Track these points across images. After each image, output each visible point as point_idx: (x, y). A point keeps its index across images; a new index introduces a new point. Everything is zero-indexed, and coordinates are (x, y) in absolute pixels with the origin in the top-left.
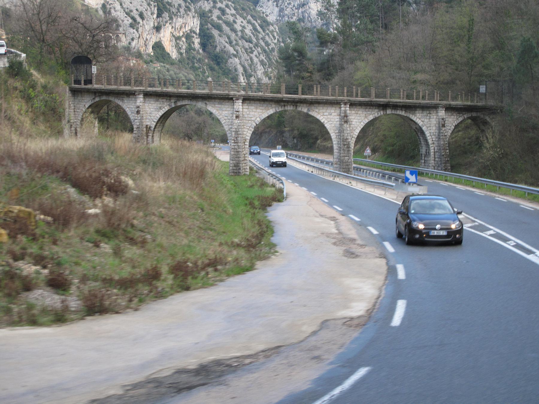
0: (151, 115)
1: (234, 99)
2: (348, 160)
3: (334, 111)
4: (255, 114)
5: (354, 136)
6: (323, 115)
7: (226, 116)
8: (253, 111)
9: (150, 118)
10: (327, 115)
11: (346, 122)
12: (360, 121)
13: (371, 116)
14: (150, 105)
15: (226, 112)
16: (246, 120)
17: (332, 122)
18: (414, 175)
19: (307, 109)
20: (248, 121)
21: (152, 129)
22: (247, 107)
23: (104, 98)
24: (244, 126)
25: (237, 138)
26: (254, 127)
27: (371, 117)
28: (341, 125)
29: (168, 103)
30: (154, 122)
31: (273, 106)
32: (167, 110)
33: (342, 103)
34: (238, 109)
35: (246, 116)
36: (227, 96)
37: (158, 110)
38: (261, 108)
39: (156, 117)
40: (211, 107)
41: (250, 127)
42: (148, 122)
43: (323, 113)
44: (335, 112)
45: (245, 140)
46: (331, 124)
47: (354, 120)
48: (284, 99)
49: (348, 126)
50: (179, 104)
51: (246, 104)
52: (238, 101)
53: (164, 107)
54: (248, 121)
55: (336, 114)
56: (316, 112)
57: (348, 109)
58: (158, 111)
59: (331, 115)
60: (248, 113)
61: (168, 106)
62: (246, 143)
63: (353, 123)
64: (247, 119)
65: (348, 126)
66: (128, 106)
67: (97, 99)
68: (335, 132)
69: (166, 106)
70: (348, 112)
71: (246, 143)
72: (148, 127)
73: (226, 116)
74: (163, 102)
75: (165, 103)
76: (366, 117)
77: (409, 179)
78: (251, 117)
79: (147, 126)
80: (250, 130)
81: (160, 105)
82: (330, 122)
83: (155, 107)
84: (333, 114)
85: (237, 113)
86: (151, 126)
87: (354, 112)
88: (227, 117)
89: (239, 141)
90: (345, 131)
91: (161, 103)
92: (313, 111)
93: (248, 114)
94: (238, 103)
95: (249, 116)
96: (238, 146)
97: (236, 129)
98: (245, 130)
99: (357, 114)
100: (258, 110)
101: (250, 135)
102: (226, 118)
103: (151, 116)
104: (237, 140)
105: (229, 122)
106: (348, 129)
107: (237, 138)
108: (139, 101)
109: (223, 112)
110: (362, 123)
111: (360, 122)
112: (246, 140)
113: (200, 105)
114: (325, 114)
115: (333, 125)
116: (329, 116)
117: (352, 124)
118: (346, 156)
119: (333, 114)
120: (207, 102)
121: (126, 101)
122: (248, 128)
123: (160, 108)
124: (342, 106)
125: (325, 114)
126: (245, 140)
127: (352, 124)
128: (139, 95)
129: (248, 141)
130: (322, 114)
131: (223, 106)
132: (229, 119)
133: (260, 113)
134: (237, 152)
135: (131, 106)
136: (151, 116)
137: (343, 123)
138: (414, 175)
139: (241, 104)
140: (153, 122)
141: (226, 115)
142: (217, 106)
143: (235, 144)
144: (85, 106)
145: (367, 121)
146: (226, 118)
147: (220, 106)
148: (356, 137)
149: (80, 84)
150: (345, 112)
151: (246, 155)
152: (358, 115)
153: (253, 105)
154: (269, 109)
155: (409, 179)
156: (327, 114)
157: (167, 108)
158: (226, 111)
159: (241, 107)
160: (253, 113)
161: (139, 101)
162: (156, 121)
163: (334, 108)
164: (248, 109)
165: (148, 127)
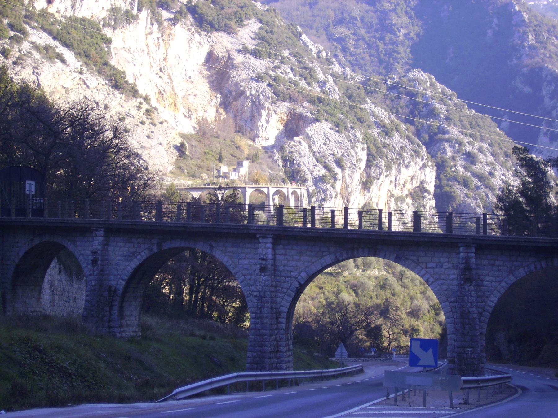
0: (118, 267)
1: (257, 236)
2: (472, 353)
3: (446, 260)
4: (299, 264)
5: (487, 308)
6: (426, 268)
7: (245, 269)
8: (293, 261)
9: (116, 273)
10: (433, 268)
11: (468, 280)
12: (498, 279)
13: (521, 270)
14: (116, 248)
15: (246, 261)
16: (281, 276)
17: (442, 281)
18: (430, 351)
19: (395, 255)
20: (285, 277)
21: (120, 292)
22: (283, 252)
23: (47, 238)
24: (276, 286)
25: (261, 308)
26: (295, 289)
27: (522, 272)
28: (461, 286)
29: (147, 246)
30: (123, 280)
31: (332, 249)
32: (144, 258)
33: (460, 245)
34: (265, 254)
35: (281, 268)
36: (245, 231)
37: (129, 259)
38: (308, 253)
39: (125, 272)
40: (219, 252)
41: (288, 289)
42: (114, 280)
43: (426, 263)
44: (448, 262)
45: (280, 313)
46: (442, 284)
47: (487, 278)
48: (349, 236)
49: (472, 288)
50: (167, 246)
51: (281, 247)
52: (265, 241)
53: (140, 253)
54: (285, 277)
55: (451, 265)
56: (413, 261)
57: (473, 255)
58: (131, 260)
59: (441, 267)
60: (284, 262)
61: (146, 251)
62: (280, 320)
63: (485, 283)
64: (283, 274)
65: (472, 288)
66: (82, 252)
67: (37, 241)
68: (450, 300)
69: (143, 251)
70: (473, 260)
71: (280, 320)
72: (113, 289)
73: (245, 269)
74: (138, 243)
75: (143, 246)
76: (511, 272)
77: (419, 359)
78: (291, 271)
79: (111, 287)
80: (288, 295)
81: (134, 250)
82: (439, 282)
83: (125, 254)
84: (446, 266)
85: (264, 262)
86: (118, 287)
87: (486, 262)
88: (248, 270)
89: (265, 315)
90: (466, 298)
91: (136, 245)
92: (407, 259)
93: (285, 266)
94: (266, 243)
95: (286, 268)
96: (262, 323)
97: (259, 292)
98: (278, 294)
99: (493, 265)
100: (303, 258)
101: (289, 304)
102: (244, 272)
103: (117, 270)
104: (261, 312)
105: (250, 279)
106: (473, 293)
107: (261, 308)
108: (97, 242)
109: (240, 261)
110: (503, 284)
111: (500, 282)
112: (280, 314)
113: (201, 247)
114: (430, 265)
115: (444, 287)
116: (437, 270)
117: (483, 285)
118: (467, 347)
119: (446, 266)
120: (214, 244)
121: (79, 243)
122: (285, 290)
123: (134, 255)
124: (461, 249)
125: (430, 265)
126: (280, 313)
127: (483, 285)
128: (96, 230)
129: (284, 315)
130: (424, 266)
131: (240, 250)
132: (251, 275)
133: (306, 264)
134: (259, 335)
135: (87, 252)
136: (117, 270)
137: (463, 282)
138: (430, 351)
139: (270, 245)
140: (120, 281)
141: (246, 267)
142: (229, 249)
143: (257, 321)
144: (18, 253)
145: (512, 279)
146: (244, 272)
147: (234, 249)
148: (491, 310)
149: (9, 215)
150: (467, 260)
151: (280, 343)
152: (495, 268)
153: (295, 247)
154: (323, 256)
155: (419, 359)
156: (433, 265)
157: (144, 255)
158: (245, 258)
159: (270, 251)
160: (294, 263)
161: (97, 242)
162: (126, 278)
163: (445, 255)
164: (285, 255)
165: (113, 289)
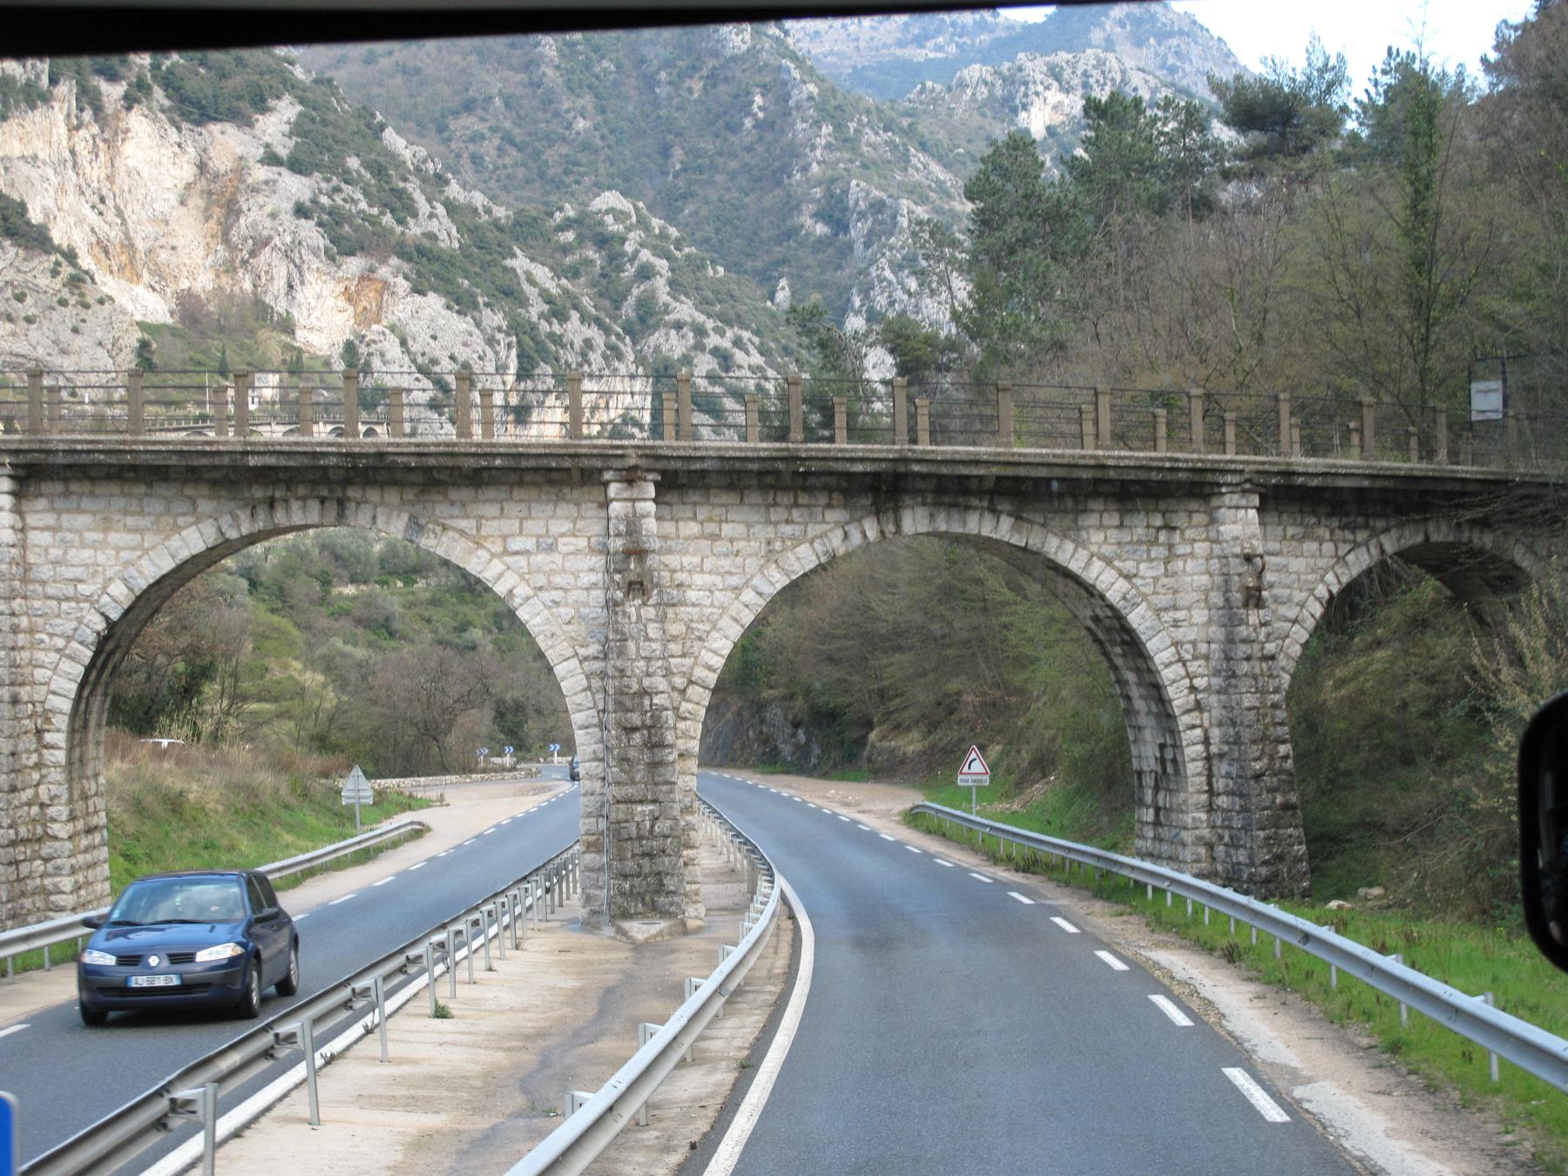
3: (566, 526)
4: (101, 558)
5: (700, 673)
6: (506, 552)
8: (83, 545)
10: (526, 553)
11: (638, 587)
12: (733, 581)
13: (803, 550)
19: (405, 517)
20: (59, 600)
22: (49, 519)
24: (32, 631)
26: (92, 638)
27: (804, 558)
28: (611, 605)
31: (205, 506)
33: (608, 476)
35: (45, 572)
38: (130, 521)
41: (69, 639)
43: (504, 538)
47: (698, 579)
48: (252, 461)
49: (650, 612)
51: (42, 503)
56: (462, 533)
57: (651, 507)
59: (551, 548)
60: (55, 553)
62: (49, 737)
64: (50, 590)
65: (650, 612)
68: (582, 652)
70: (650, 525)
71: (49, 737)
76: (770, 556)
80: (71, 658)
82: (547, 596)
87: (692, 528)
90: (631, 645)
92: (445, 528)
93: (56, 563)
98: (40, 656)
99: (715, 537)
100: (114, 537)
101: (74, 687)
106: (653, 630)
110: (748, 596)
111: (737, 590)
112: (48, 720)
114: (516, 544)
115: (565, 612)
116: (540, 559)
117: (682, 603)
118: (641, 802)
122: (60, 643)
124: (613, 489)
125: (516, 544)
129: (62, 722)
130: (497, 548)
133: (125, 555)
137: (619, 595)
145: (778, 580)
148: (712, 679)
150: (632, 526)
151: (51, 811)
152: (721, 547)
153: (86, 503)
154: (177, 529)
156: (530, 543)
163: (565, 509)
